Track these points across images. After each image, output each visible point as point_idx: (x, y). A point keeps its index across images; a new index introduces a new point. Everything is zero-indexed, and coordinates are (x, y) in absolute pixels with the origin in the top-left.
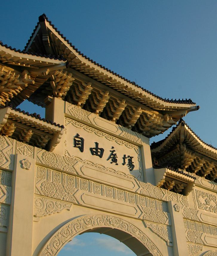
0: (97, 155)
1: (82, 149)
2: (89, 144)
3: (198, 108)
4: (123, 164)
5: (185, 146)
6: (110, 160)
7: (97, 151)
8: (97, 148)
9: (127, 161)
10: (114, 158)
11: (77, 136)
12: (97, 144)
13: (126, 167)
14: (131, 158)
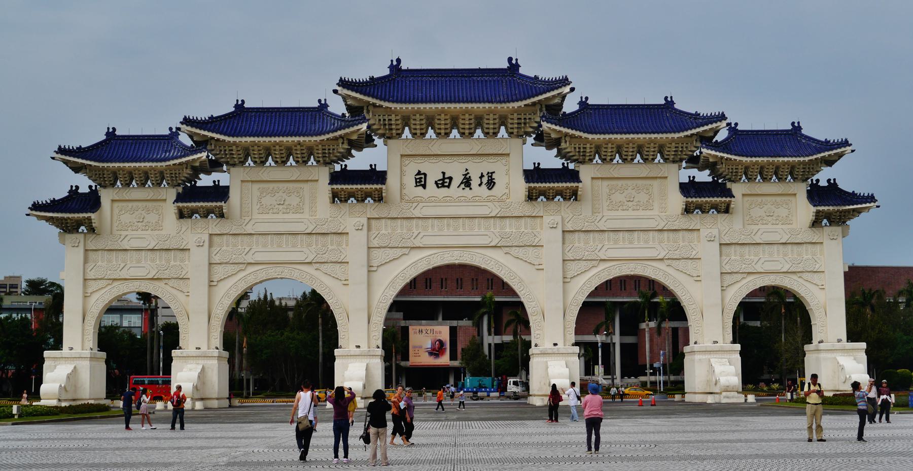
0: (443, 186)
1: (424, 186)
2: (433, 177)
3: (572, 90)
4: (480, 185)
5: (568, 139)
6: (463, 186)
7: (444, 182)
8: (444, 178)
9: (485, 180)
10: (467, 182)
11: (419, 173)
12: (444, 173)
13: (484, 187)
14: (491, 175)
